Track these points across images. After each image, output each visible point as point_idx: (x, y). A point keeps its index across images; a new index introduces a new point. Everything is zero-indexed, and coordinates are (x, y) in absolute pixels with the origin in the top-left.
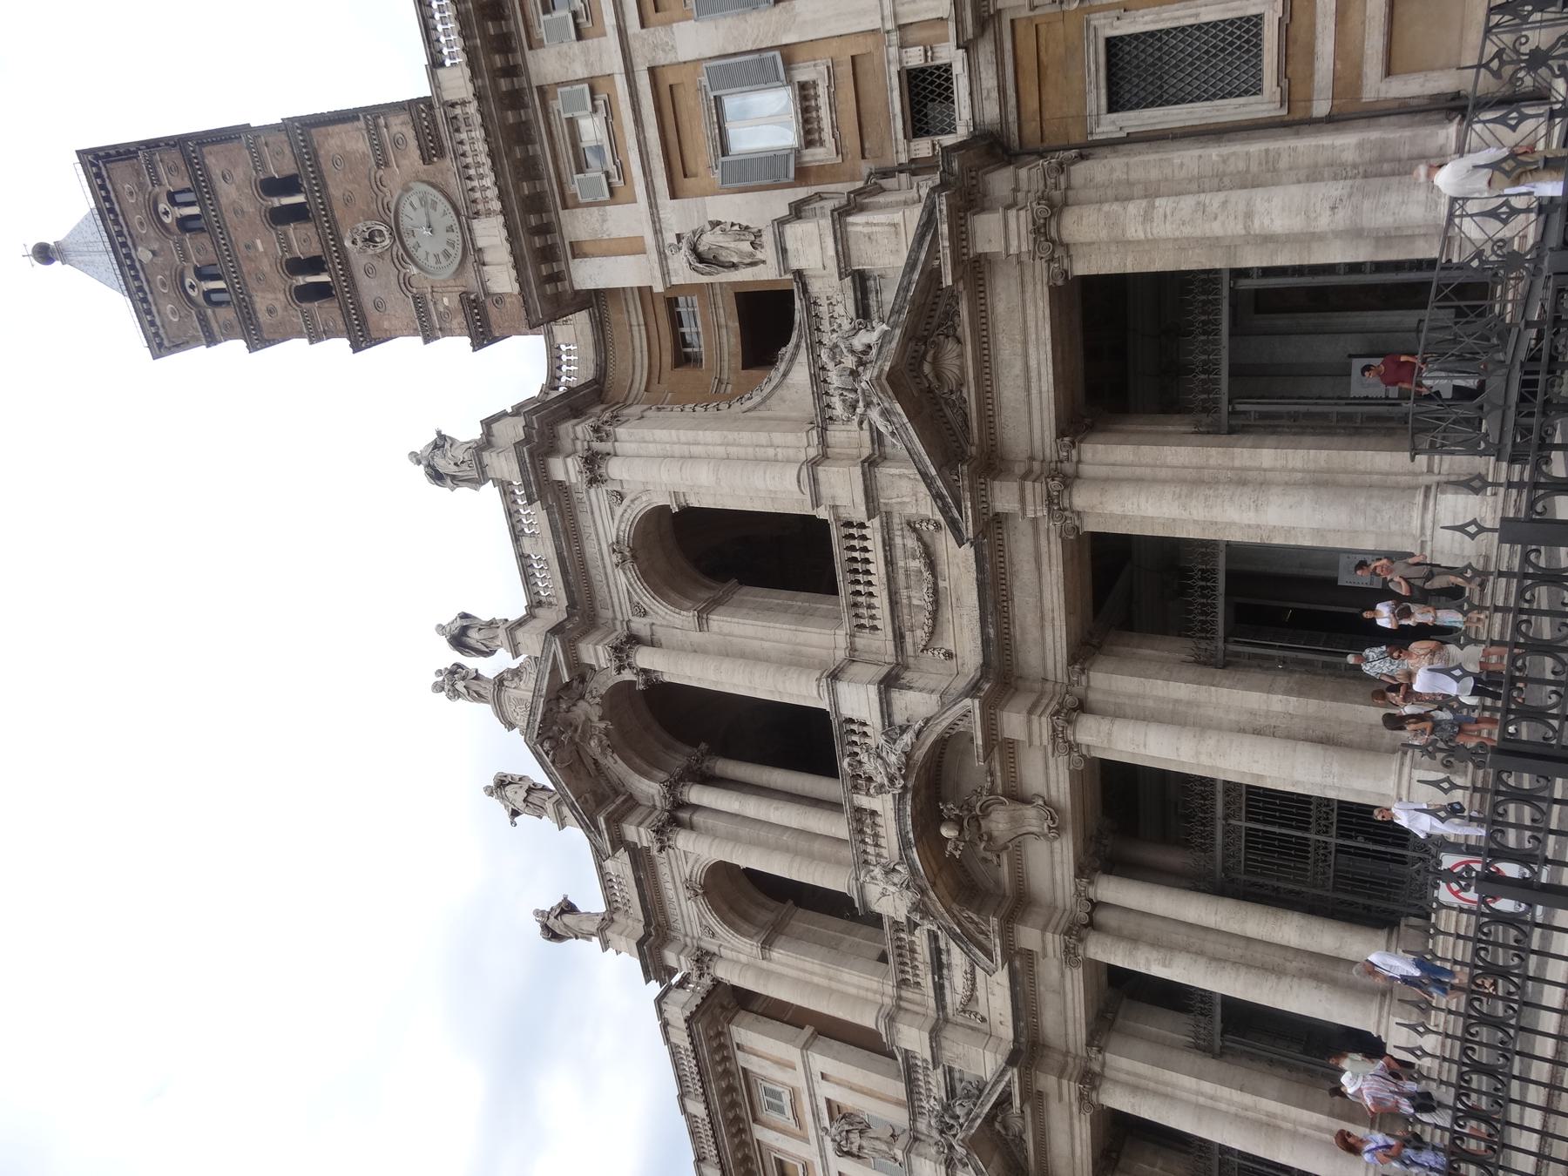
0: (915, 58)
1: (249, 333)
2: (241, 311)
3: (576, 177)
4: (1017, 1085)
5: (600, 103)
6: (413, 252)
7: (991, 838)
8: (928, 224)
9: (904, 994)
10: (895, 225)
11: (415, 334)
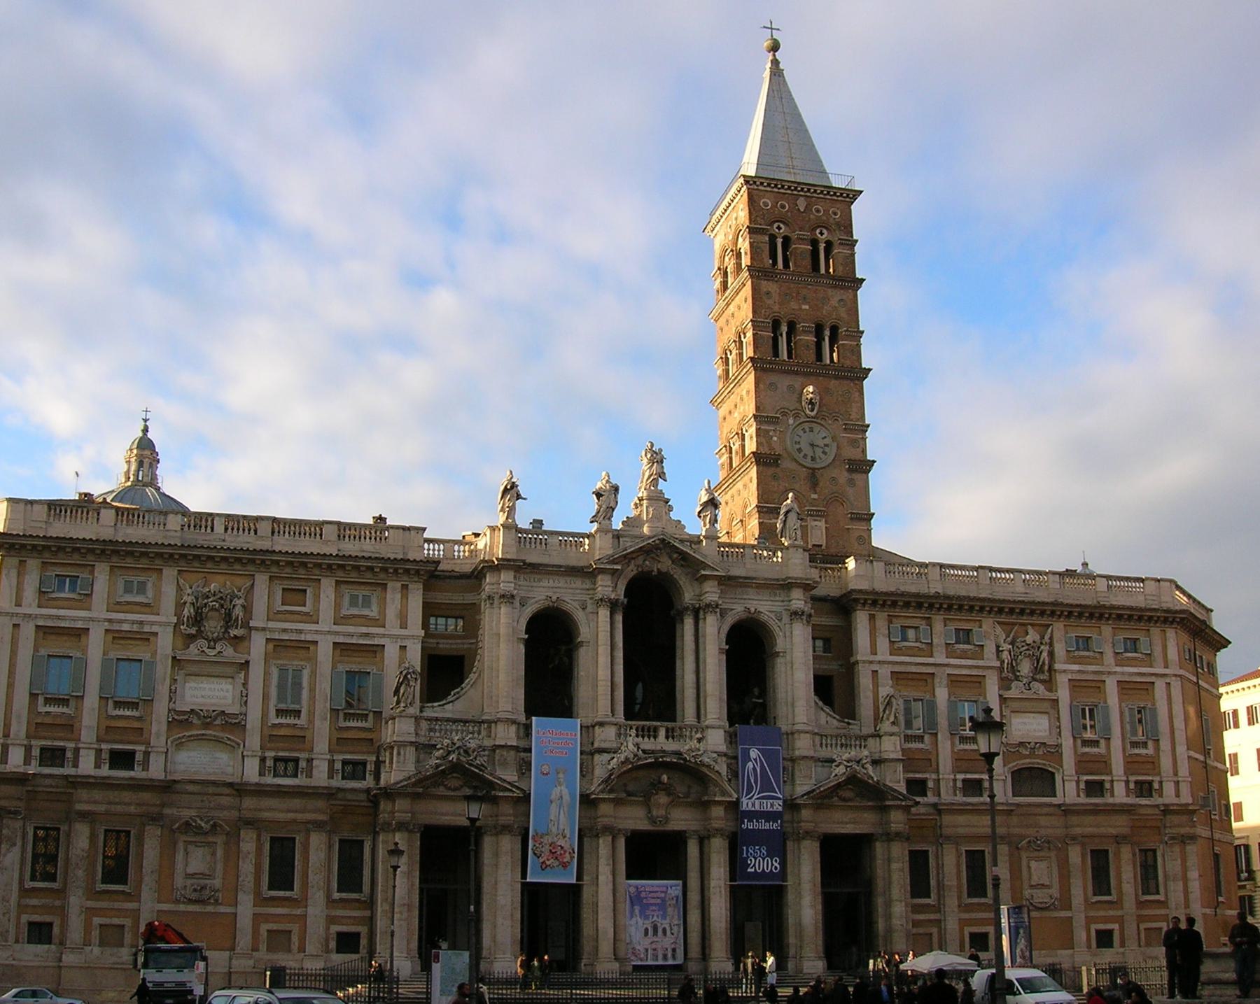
0: (930, 784)
1: (758, 271)
4: (511, 795)
5: (924, 646)
6: (800, 428)
7: (657, 794)
9: (521, 726)
10: (899, 782)
11: (757, 408)
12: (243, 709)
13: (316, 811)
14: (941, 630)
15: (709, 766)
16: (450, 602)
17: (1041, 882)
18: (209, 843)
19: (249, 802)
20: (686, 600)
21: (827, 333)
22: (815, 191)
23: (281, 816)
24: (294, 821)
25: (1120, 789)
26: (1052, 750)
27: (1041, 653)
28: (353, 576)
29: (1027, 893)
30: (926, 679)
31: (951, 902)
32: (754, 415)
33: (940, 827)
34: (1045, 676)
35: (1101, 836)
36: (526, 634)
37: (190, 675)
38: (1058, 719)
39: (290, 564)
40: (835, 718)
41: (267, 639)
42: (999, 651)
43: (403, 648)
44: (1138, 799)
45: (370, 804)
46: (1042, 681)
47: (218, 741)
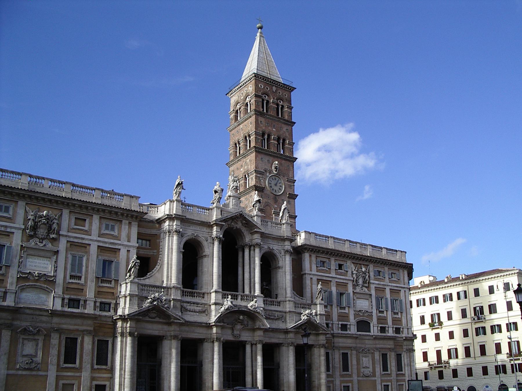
1: (258, 112)
3: (319, 260)
5: (328, 269)
10: (324, 324)
11: (256, 167)
12: (55, 274)
13: (88, 326)
14: (333, 264)
15: (259, 313)
16: (145, 233)
17: (366, 366)
18: (35, 339)
19: (56, 320)
20: (247, 241)
21: (281, 141)
22: (279, 85)
23: (72, 327)
24: (77, 330)
25: (391, 330)
26: (370, 314)
28: (108, 216)
29: (362, 370)
31: (338, 373)
32: (255, 170)
33: (334, 343)
34: (367, 285)
36: (183, 249)
37: (29, 255)
38: (371, 302)
39: (80, 207)
40: (297, 296)
41: (67, 241)
43: (128, 251)
44: (396, 335)
45: (112, 323)
46: (366, 287)
47: (41, 288)
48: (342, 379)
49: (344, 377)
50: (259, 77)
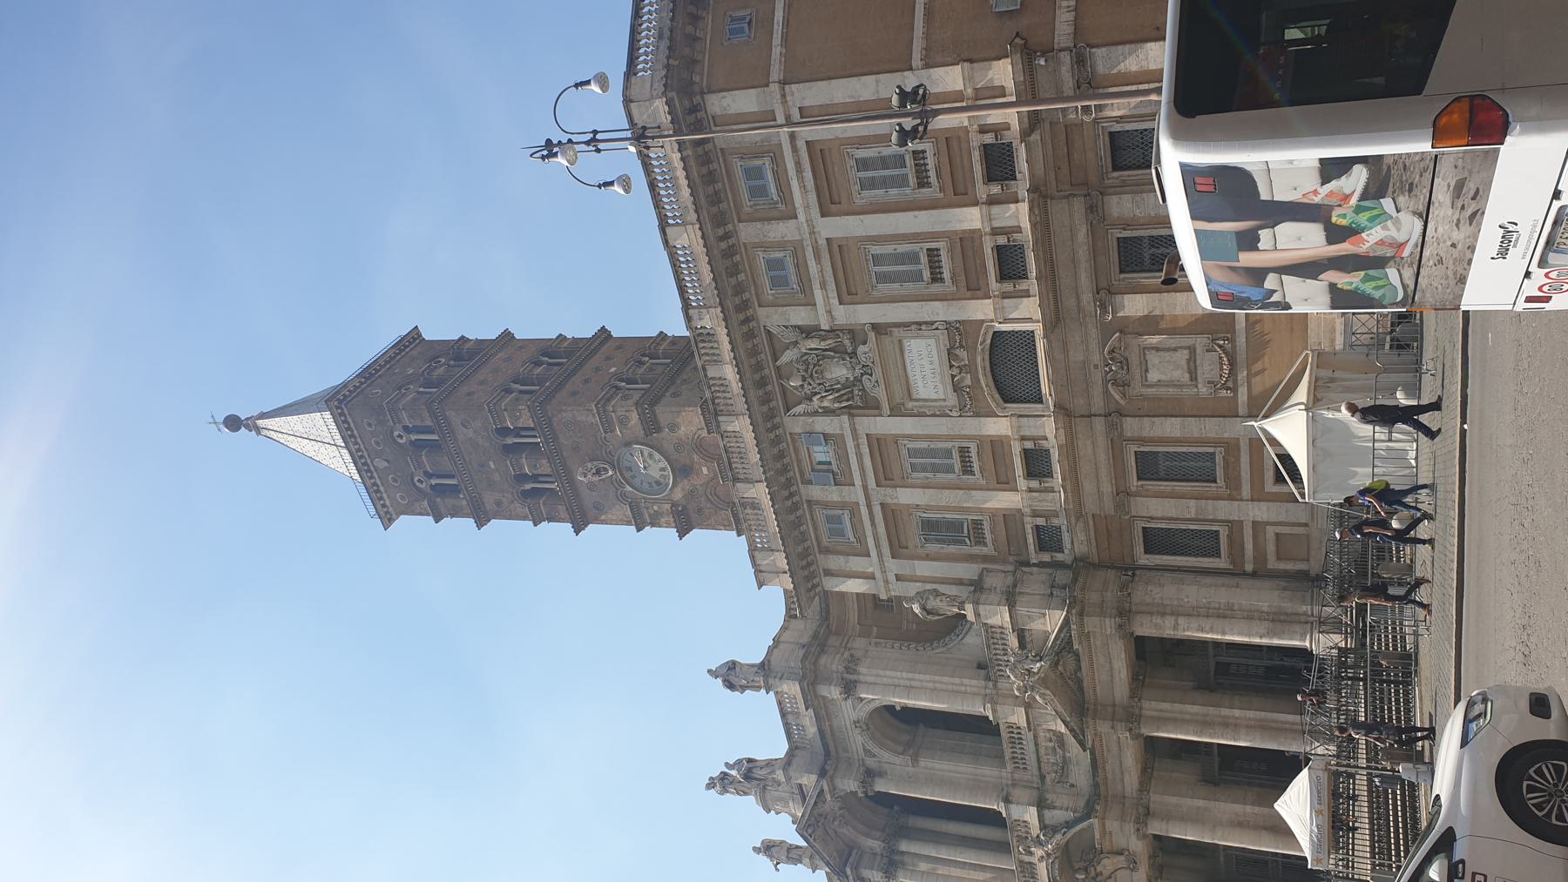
2: (473, 505)
8: (1066, 622)
11: (629, 523)
17: (1184, 363)
27: (811, 349)
29: (1204, 390)
30: (892, 515)
31: (1225, 510)
35: (1094, 253)
38: (904, 325)
42: (828, 412)
44: (1019, 176)
48: (1246, 491)
49: (1239, 476)
50: (385, 510)
